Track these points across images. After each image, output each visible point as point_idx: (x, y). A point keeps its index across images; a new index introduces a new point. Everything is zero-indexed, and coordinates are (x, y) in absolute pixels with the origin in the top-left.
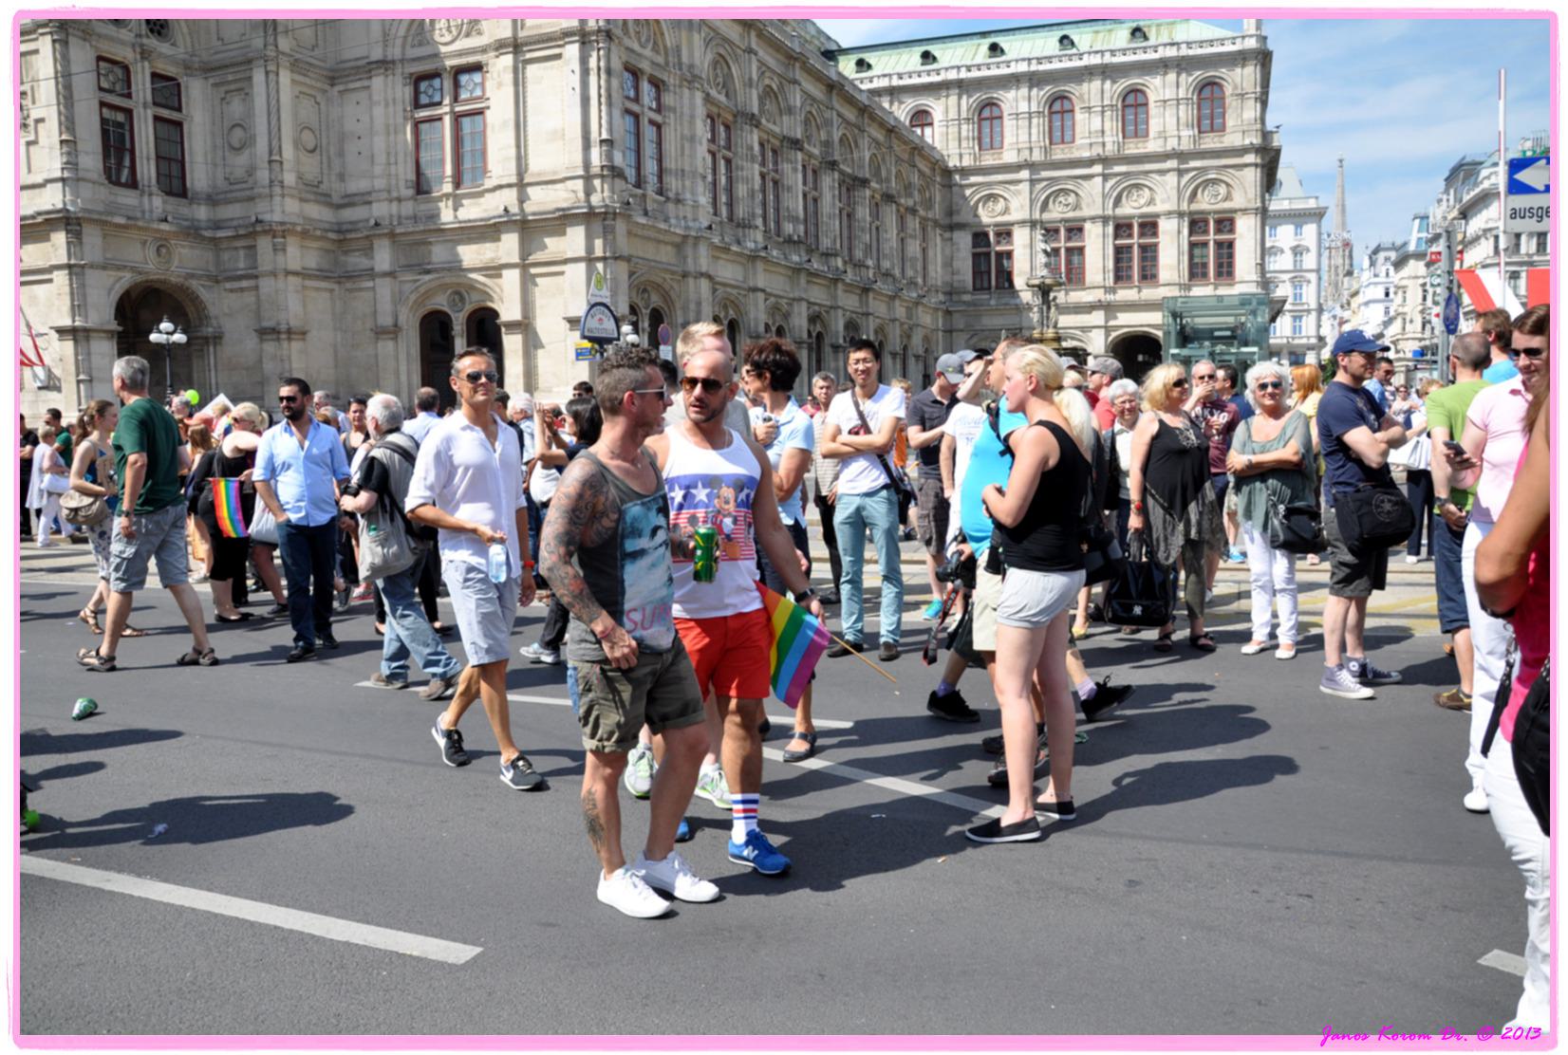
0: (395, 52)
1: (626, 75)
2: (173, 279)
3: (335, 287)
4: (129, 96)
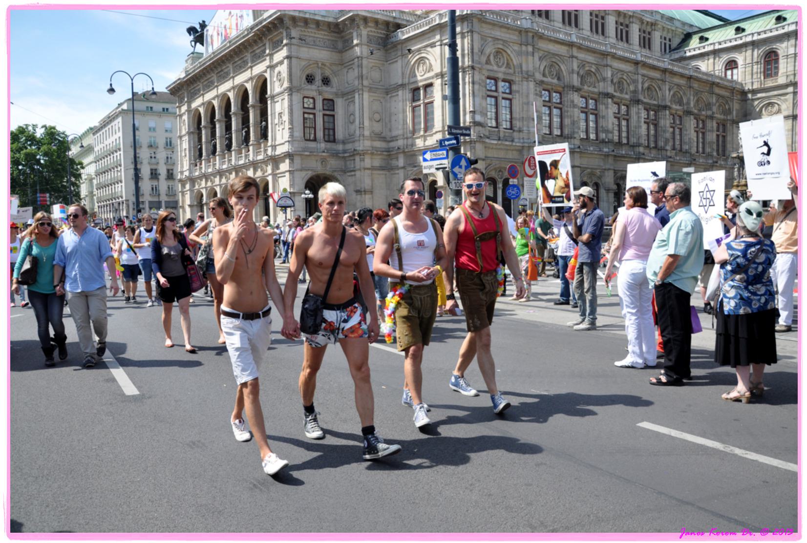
0: (406, 81)
1: (488, 81)
2: (328, 173)
3: (387, 173)
4: (314, 108)
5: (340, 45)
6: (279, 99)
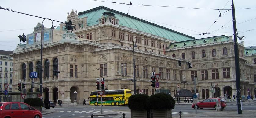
5: (79, 51)
6: (63, 65)
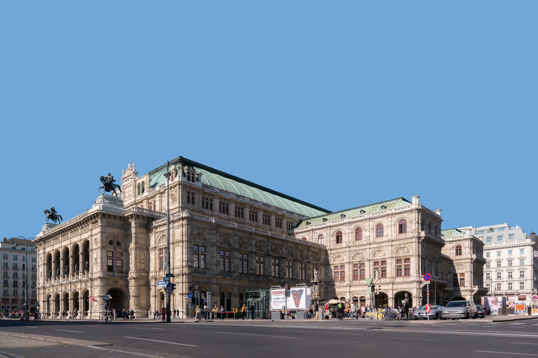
1: (194, 247)
